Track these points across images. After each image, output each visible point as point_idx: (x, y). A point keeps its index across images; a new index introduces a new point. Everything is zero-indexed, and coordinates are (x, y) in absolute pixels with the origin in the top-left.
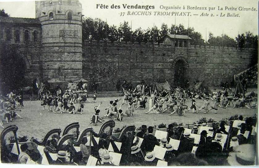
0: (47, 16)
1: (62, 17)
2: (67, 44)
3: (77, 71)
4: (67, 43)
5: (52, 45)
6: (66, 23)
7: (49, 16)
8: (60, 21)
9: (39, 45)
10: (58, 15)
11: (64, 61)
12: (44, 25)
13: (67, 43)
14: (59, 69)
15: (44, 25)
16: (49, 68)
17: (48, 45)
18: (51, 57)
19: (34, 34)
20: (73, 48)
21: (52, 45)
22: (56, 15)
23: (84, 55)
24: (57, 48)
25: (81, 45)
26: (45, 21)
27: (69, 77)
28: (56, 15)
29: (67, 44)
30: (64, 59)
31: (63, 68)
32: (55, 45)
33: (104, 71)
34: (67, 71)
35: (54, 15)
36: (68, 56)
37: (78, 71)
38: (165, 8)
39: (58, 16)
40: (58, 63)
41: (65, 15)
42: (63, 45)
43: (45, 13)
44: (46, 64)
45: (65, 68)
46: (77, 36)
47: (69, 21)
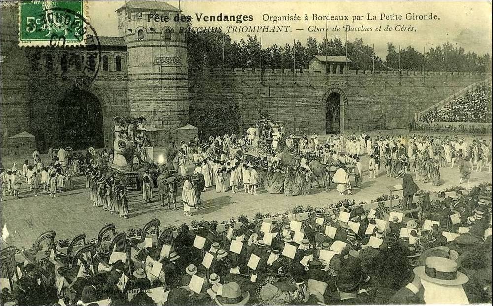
0: (135, 34)
1: (158, 37)
2: (166, 76)
3: (180, 114)
4: (164, 74)
5: (143, 77)
6: (164, 46)
7: (137, 34)
8: (155, 43)
9: (125, 77)
10: (150, 33)
11: (162, 100)
12: (131, 47)
13: (164, 74)
14: (155, 112)
15: (131, 47)
16: (140, 110)
17: (137, 77)
18: (142, 94)
19: (118, 60)
20: (175, 81)
21: (143, 77)
22: (147, 33)
23: (191, 90)
24: (151, 81)
25: (186, 77)
26: (133, 42)
27: (169, 122)
28: (147, 33)
29: (166, 76)
30: (160, 97)
31: (160, 110)
32: (148, 77)
33: (222, 112)
34: (166, 114)
35: (145, 33)
36: (167, 92)
37: (182, 113)
38: (325, 18)
39: (151, 35)
40: (153, 103)
41: (161, 33)
42: (158, 77)
43: (131, 31)
44: (137, 103)
45: (163, 110)
46: (180, 63)
47: (168, 42)
